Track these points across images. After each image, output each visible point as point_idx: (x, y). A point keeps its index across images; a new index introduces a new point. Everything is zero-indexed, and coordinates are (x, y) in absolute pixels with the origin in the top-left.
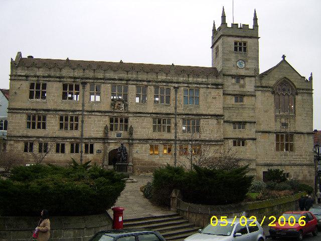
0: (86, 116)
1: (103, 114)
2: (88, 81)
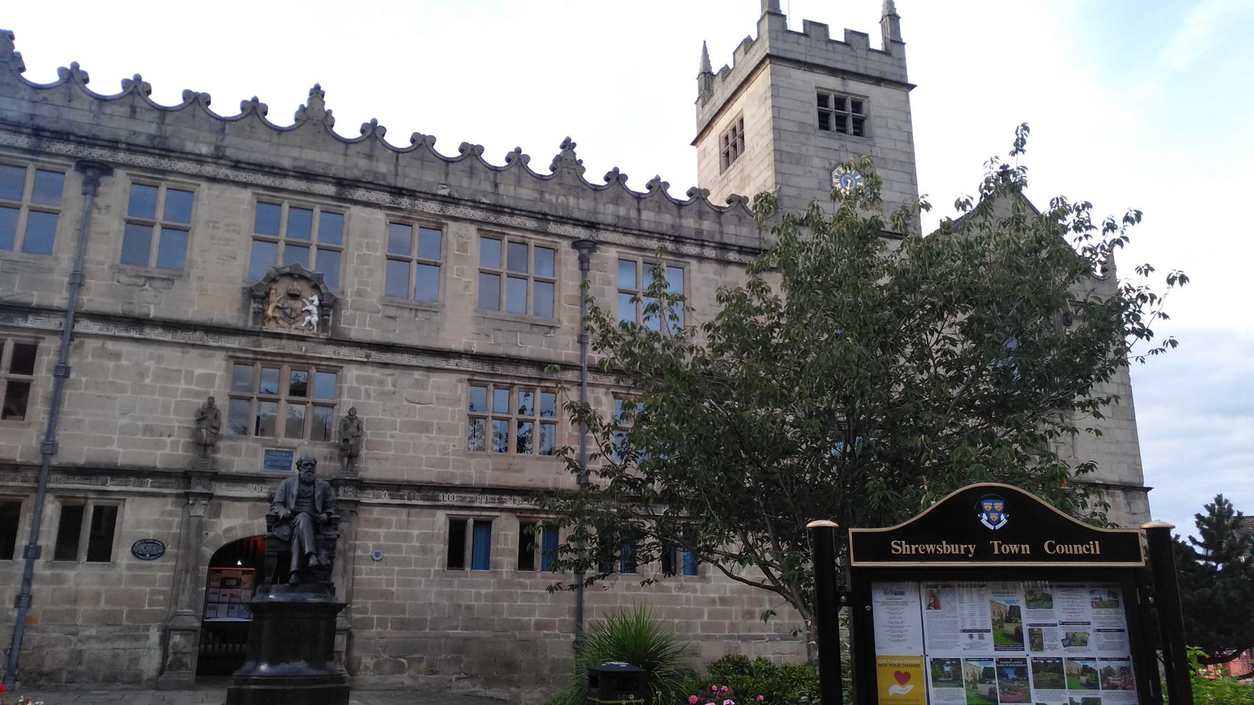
0: (90, 344)
1: (197, 337)
2: (121, 157)
